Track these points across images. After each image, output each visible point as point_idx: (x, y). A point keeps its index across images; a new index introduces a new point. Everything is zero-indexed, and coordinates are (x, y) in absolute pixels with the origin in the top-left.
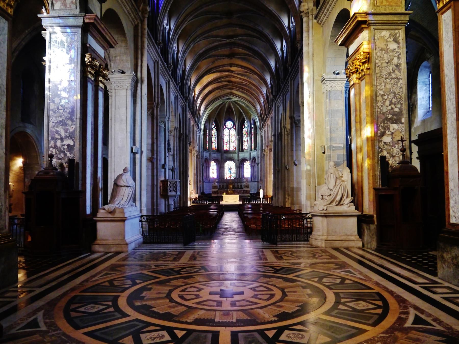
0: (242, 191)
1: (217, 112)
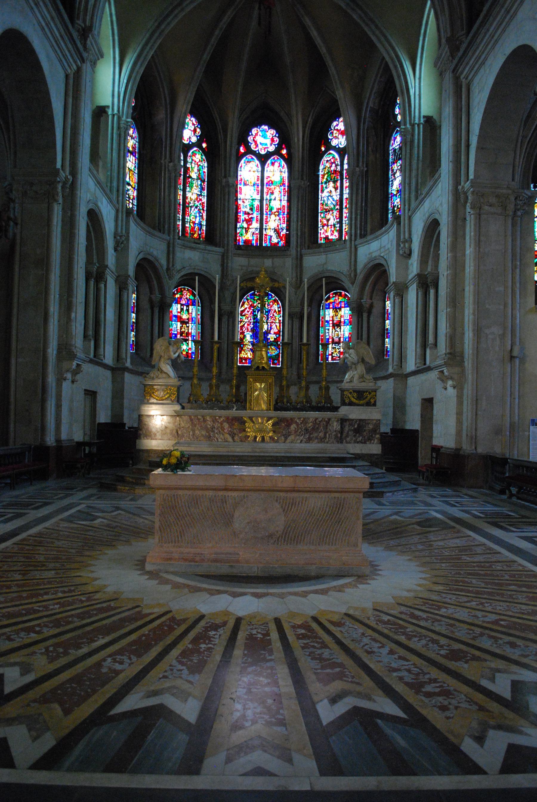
0: (336, 426)
1: (210, 49)
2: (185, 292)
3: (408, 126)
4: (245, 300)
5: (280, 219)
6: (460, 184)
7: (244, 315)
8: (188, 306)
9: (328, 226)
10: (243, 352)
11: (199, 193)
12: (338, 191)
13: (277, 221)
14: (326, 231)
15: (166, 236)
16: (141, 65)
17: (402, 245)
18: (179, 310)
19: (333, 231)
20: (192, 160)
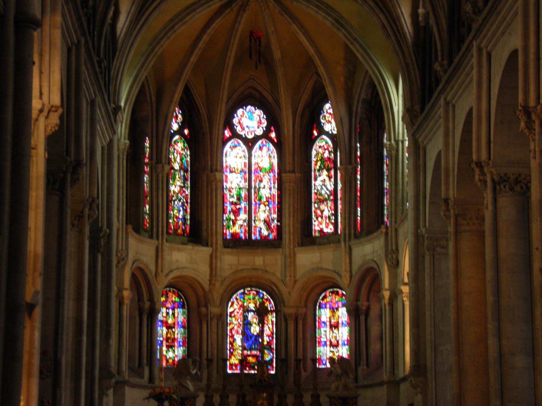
2: (170, 294)
3: (393, 142)
4: (235, 300)
5: (270, 210)
6: (420, 228)
7: (234, 316)
8: (173, 309)
9: (322, 218)
10: (233, 357)
11: (182, 185)
12: (333, 180)
13: (267, 211)
14: (321, 223)
15: (154, 242)
16: (136, 87)
17: (390, 256)
18: (165, 315)
19: (328, 224)
20: (174, 149)
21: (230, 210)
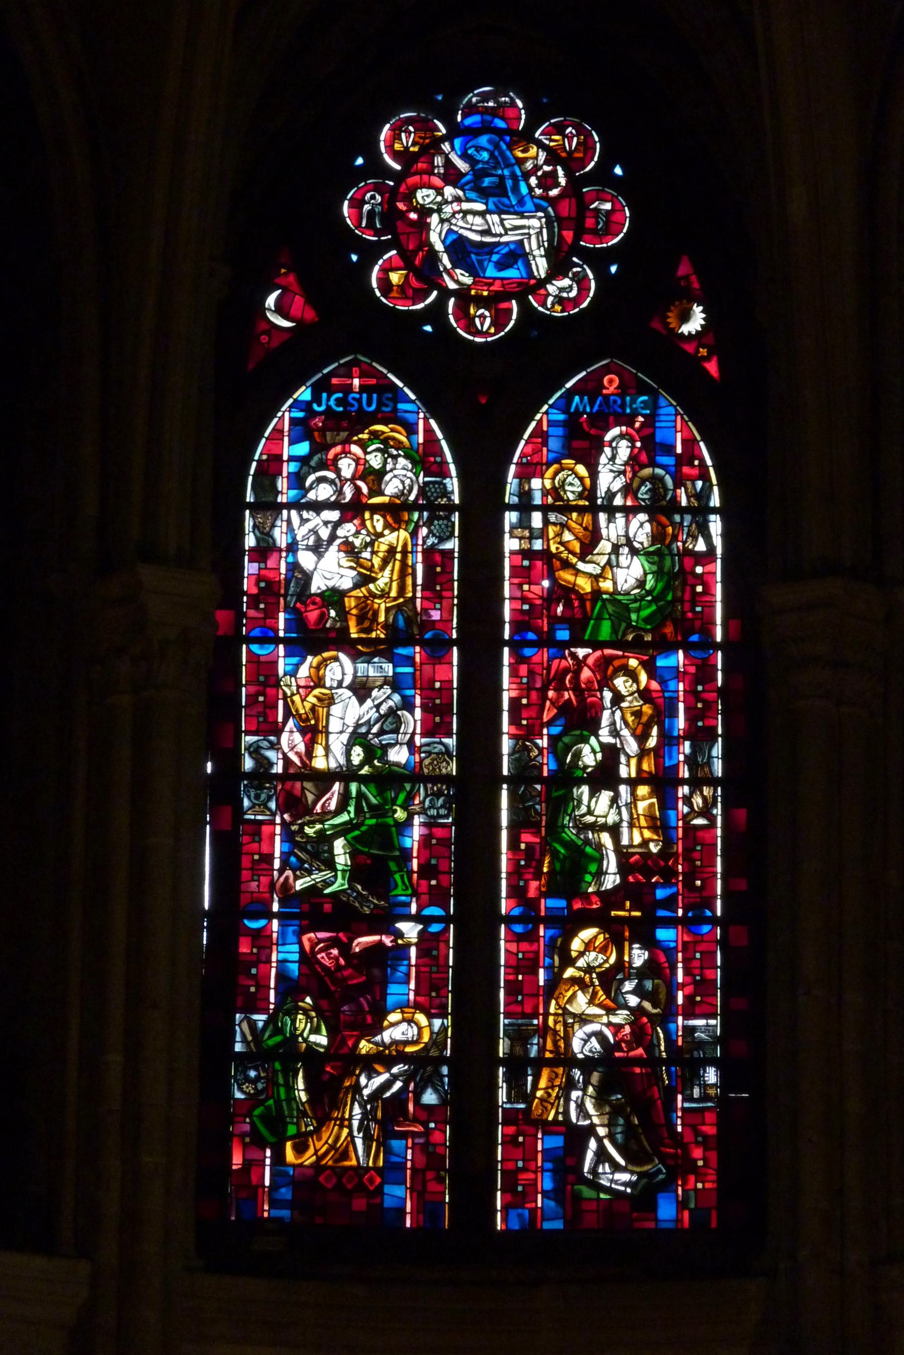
21: (294, 969)
